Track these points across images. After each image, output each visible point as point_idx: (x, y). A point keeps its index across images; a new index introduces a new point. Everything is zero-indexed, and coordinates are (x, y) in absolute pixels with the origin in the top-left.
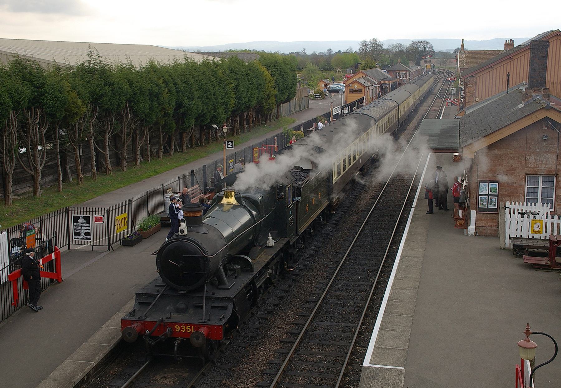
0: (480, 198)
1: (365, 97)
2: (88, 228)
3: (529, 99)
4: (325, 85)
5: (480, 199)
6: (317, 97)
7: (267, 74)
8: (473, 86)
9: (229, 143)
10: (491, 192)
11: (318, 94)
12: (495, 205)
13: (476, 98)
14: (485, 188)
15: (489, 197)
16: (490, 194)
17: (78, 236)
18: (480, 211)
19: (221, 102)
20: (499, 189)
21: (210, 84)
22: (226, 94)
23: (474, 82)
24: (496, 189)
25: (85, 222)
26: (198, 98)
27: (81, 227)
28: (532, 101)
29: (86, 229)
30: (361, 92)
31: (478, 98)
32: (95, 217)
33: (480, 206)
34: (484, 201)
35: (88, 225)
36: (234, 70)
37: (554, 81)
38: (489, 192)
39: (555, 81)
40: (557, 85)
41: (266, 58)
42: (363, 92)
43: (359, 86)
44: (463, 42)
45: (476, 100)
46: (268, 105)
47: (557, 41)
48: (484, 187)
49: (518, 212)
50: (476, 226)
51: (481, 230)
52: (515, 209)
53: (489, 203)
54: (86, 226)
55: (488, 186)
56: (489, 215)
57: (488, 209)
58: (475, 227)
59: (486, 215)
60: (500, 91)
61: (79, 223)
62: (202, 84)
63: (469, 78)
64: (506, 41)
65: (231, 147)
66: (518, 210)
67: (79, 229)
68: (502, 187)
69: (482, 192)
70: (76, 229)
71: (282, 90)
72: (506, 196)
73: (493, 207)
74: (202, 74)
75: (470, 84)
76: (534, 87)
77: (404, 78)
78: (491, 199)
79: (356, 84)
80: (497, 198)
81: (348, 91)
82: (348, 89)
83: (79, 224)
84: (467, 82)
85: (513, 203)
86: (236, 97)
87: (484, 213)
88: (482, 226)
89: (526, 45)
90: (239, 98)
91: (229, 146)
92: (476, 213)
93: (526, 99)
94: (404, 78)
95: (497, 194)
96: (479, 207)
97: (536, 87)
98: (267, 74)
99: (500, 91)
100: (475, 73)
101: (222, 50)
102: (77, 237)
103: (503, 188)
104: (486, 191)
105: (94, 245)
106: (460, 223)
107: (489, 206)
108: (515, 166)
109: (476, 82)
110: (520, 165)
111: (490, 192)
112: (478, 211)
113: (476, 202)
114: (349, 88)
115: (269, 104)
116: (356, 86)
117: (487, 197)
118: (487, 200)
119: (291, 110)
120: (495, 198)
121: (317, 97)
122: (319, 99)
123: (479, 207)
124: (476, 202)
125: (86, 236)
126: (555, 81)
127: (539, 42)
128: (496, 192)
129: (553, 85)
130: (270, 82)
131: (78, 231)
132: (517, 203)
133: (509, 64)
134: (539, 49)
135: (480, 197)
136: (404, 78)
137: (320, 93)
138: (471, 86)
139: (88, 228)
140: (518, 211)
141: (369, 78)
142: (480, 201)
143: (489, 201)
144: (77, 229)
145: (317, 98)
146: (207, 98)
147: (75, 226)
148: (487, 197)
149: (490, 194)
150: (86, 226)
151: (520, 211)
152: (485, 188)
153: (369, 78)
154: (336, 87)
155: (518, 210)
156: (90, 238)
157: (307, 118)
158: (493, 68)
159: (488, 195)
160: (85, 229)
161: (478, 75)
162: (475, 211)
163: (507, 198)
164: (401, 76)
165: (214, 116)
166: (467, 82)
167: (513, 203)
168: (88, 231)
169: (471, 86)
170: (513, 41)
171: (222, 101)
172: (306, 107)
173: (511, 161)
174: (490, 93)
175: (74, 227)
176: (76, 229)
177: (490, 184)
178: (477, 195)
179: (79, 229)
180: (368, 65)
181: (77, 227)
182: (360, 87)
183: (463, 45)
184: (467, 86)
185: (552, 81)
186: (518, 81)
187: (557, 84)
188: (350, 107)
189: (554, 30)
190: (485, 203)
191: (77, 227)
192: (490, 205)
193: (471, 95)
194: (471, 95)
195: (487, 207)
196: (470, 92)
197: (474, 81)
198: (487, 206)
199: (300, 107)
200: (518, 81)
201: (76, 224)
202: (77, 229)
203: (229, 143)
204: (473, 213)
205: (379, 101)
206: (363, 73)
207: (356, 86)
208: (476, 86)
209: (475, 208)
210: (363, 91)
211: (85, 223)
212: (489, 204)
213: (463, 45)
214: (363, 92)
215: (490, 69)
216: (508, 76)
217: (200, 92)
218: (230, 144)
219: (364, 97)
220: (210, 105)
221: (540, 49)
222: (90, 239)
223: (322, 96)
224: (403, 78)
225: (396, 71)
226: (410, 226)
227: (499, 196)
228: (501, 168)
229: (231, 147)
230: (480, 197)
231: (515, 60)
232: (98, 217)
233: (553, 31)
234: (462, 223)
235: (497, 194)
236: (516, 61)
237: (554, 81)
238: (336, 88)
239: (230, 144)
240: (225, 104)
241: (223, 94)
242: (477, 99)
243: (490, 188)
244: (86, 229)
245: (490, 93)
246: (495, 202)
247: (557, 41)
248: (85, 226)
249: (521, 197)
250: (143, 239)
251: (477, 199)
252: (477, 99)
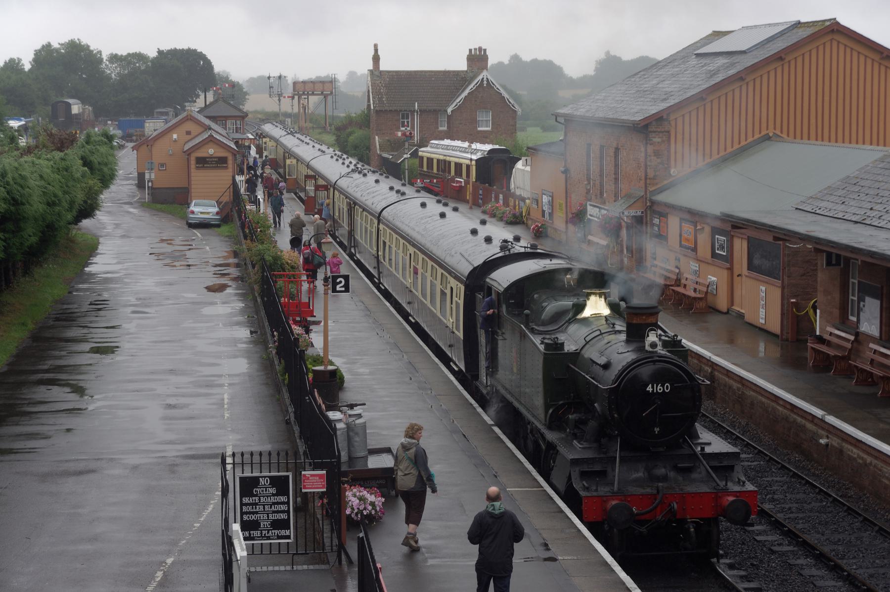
2: (283, 507)
9: (338, 281)
17: (252, 532)
25: (273, 490)
27: (262, 507)
29: (278, 512)
32: (305, 475)
35: (283, 499)
44: (376, 50)
45: (672, 173)
54: (278, 503)
61: (256, 495)
63: (654, 123)
64: (470, 50)
65: (343, 289)
67: (257, 513)
70: (246, 513)
83: (257, 498)
84: (651, 132)
91: (338, 288)
102: (250, 534)
105: (297, 554)
116: (211, 151)
125: (276, 531)
131: (253, 517)
139: (283, 507)
144: (250, 513)
147: (246, 505)
150: (278, 503)
156: (288, 533)
160: (274, 512)
161: (672, 117)
168: (283, 516)
170: (485, 50)
175: (241, 509)
176: (246, 513)
179: (257, 513)
181: (250, 509)
183: (376, 59)
189: (803, 20)
191: (250, 509)
194: (659, 161)
201: (247, 499)
202: (250, 513)
203: (338, 281)
211: (273, 495)
213: (376, 59)
218: (341, 282)
222: (288, 537)
229: (343, 289)
232: (312, 475)
239: (341, 282)
244: (278, 512)
248: (274, 504)
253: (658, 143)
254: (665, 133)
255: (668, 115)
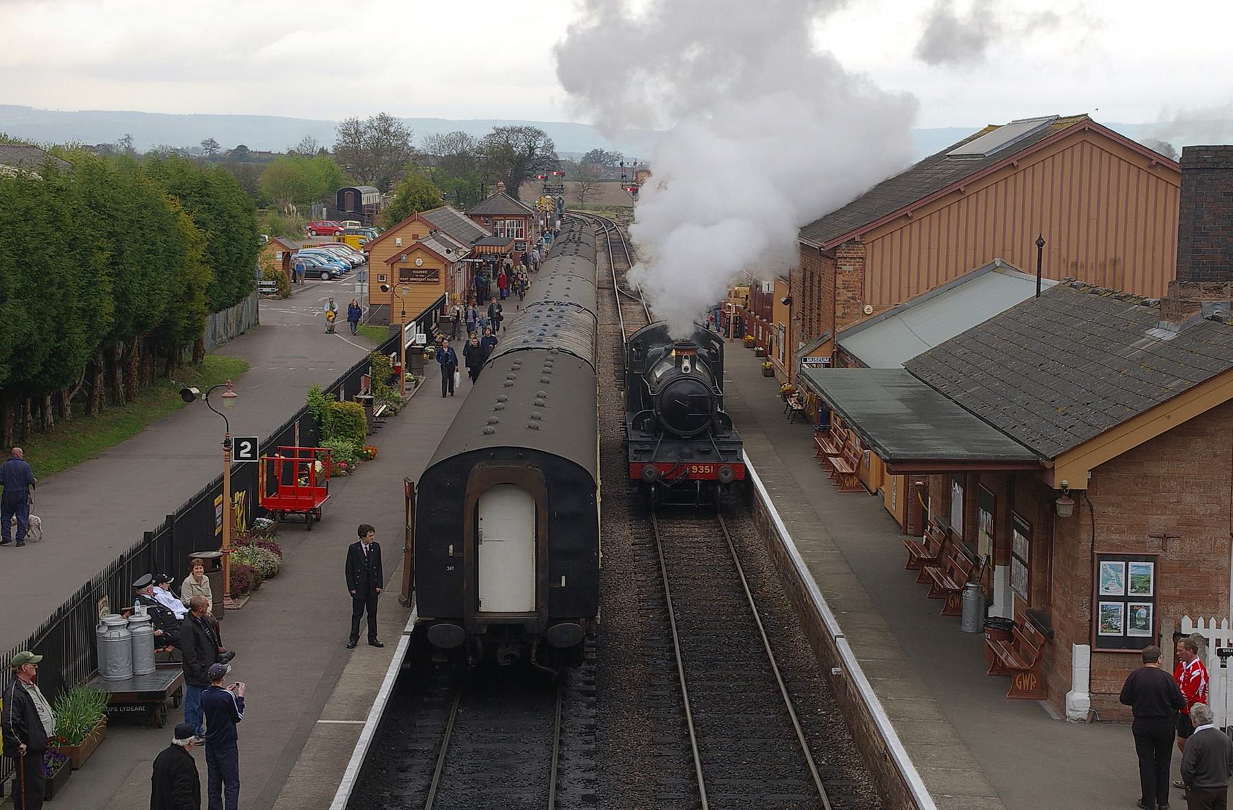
0: (1102, 606)
1: (447, 293)
3: (1193, 314)
4: (284, 253)
5: (1102, 611)
6: (264, 290)
7: (186, 221)
8: (855, 270)
9: (242, 445)
10: (1134, 590)
11: (270, 283)
12: (1145, 627)
13: (864, 303)
14: (1117, 576)
15: (1129, 604)
16: (1129, 594)
18: (1100, 645)
19: (78, 309)
20: (1158, 581)
21: (51, 250)
22: (90, 284)
23: (860, 258)
24: (1149, 581)
26: (18, 295)
28: (1201, 321)
30: (437, 280)
31: (871, 305)
33: (1102, 632)
34: (1112, 616)
36: (105, 206)
37: (1077, 260)
38: (1129, 590)
39: (1082, 259)
40: (1086, 272)
41: (172, 171)
42: (442, 281)
43: (435, 261)
46: (189, 318)
47: (1082, 147)
48: (1113, 573)
49: (1217, 648)
50: (1090, 691)
51: (1105, 706)
52: (1220, 640)
53: (1128, 623)
55: (1124, 571)
56: (1128, 660)
57: (1127, 641)
58: (1089, 697)
59: (1120, 659)
60: (933, 285)
62: (25, 250)
63: (843, 246)
65: (249, 455)
66: (1218, 642)
68: (1165, 575)
69: (1107, 589)
71: (223, 272)
72: (1178, 599)
73: (1141, 633)
74: (22, 216)
75: (848, 264)
76: (1202, 280)
77: (519, 239)
78: (1133, 610)
79: (419, 253)
80: (1151, 608)
81: (397, 275)
82: (396, 270)
84: (839, 258)
85: (1201, 621)
86: (114, 292)
87: (1113, 653)
88: (1109, 692)
89: (987, 155)
90: (121, 296)
91: (242, 454)
92: (1091, 652)
93: (1185, 315)
94: (517, 237)
95: (1151, 594)
96: (1100, 634)
97: (1209, 280)
98: (186, 221)
99: (933, 285)
100: (862, 233)
101: (45, 139)
103: (1167, 577)
104: (1118, 586)
106: (1026, 682)
107: (1128, 630)
108: (1201, 510)
109: (863, 258)
110: (1216, 508)
111: (1132, 588)
112: (1097, 647)
113: (1091, 621)
114: (397, 267)
115: (191, 312)
116: (419, 262)
117: (1123, 604)
118: (1123, 613)
119: (217, 330)
120: (1147, 608)
121: (264, 290)
122: (273, 298)
123: (1100, 634)
124: (1089, 618)
126: (1082, 259)
127: (1216, 151)
128: (1147, 589)
129: (1077, 270)
130: (195, 244)
132: (1213, 622)
133: (954, 208)
134: (1216, 171)
135: (1101, 603)
136: (519, 239)
137: (276, 278)
138: (851, 268)
140: (1216, 646)
141: (443, 235)
142: (1102, 615)
143: (1129, 617)
145: (264, 292)
146: (41, 296)
148: (1123, 604)
149: (1129, 594)
151: (1222, 647)
152: (1117, 576)
153: (443, 235)
154: (312, 261)
155: (1218, 642)
157: (276, 357)
158: (910, 218)
159: (1125, 599)
161: (869, 239)
162: (1089, 646)
163: (1180, 607)
164: (508, 231)
165: (56, 353)
166: (839, 258)
167: (1201, 621)
169: (851, 268)
171: (80, 305)
172: (252, 321)
173: (1189, 498)
174: (904, 292)
177: (1130, 566)
178: (1092, 599)
180: (417, 196)
182: (433, 265)
184: (839, 271)
185: (1072, 259)
186: (979, 255)
187: (1087, 267)
188: (423, 324)
189: (1062, 116)
190: (1115, 624)
192: (1130, 628)
193: (850, 294)
195: (1122, 634)
196: (846, 285)
197: (860, 254)
198: (1122, 630)
199: (238, 326)
200: (979, 255)
203: (242, 445)
204: (1081, 655)
205: (551, 310)
206: (425, 223)
207: (421, 262)
208: (863, 270)
209: (1087, 636)
210: (442, 276)
212: (1128, 627)
214: (442, 281)
215: (902, 223)
216: (1040, 244)
217: (19, 276)
218: (246, 447)
219: (445, 295)
220: (49, 319)
221: (1220, 170)
223: (281, 290)
224: (515, 239)
225: (496, 215)
226: (879, 697)
227: (1158, 603)
228: (1163, 517)
229: (249, 455)
230: (1101, 603)
231: (970, 197)
233: (1058, 118)
234: (1032, 683)
235: (1151, 594)
236: (973, 199)
237: (1077, 260)
238: (312, 265)
239: (246, 447)
240: (89, 314)
241: (83, 283)
242: (868, 309)
243: (1130, 576)
245: (904, 292)
246: (1147, 620)
247: (1082, 147)
249: (1220, 604)
250: (73, 772)
251: (1093, 609)
252: (868, 309)
253: (849, 272)
254: (858, 260)
255: (862, 236)
